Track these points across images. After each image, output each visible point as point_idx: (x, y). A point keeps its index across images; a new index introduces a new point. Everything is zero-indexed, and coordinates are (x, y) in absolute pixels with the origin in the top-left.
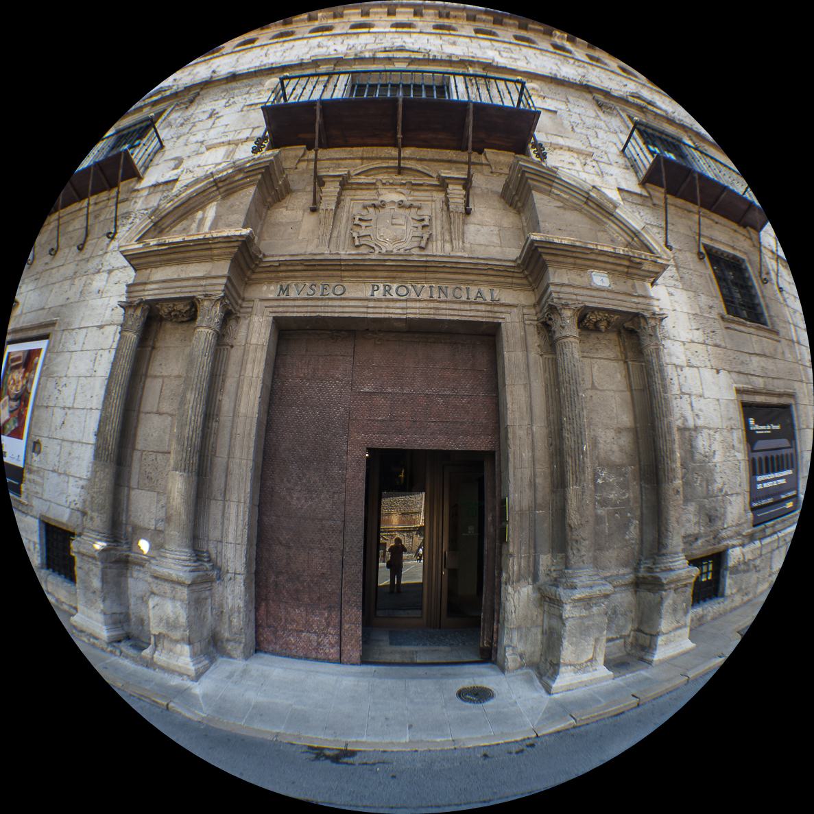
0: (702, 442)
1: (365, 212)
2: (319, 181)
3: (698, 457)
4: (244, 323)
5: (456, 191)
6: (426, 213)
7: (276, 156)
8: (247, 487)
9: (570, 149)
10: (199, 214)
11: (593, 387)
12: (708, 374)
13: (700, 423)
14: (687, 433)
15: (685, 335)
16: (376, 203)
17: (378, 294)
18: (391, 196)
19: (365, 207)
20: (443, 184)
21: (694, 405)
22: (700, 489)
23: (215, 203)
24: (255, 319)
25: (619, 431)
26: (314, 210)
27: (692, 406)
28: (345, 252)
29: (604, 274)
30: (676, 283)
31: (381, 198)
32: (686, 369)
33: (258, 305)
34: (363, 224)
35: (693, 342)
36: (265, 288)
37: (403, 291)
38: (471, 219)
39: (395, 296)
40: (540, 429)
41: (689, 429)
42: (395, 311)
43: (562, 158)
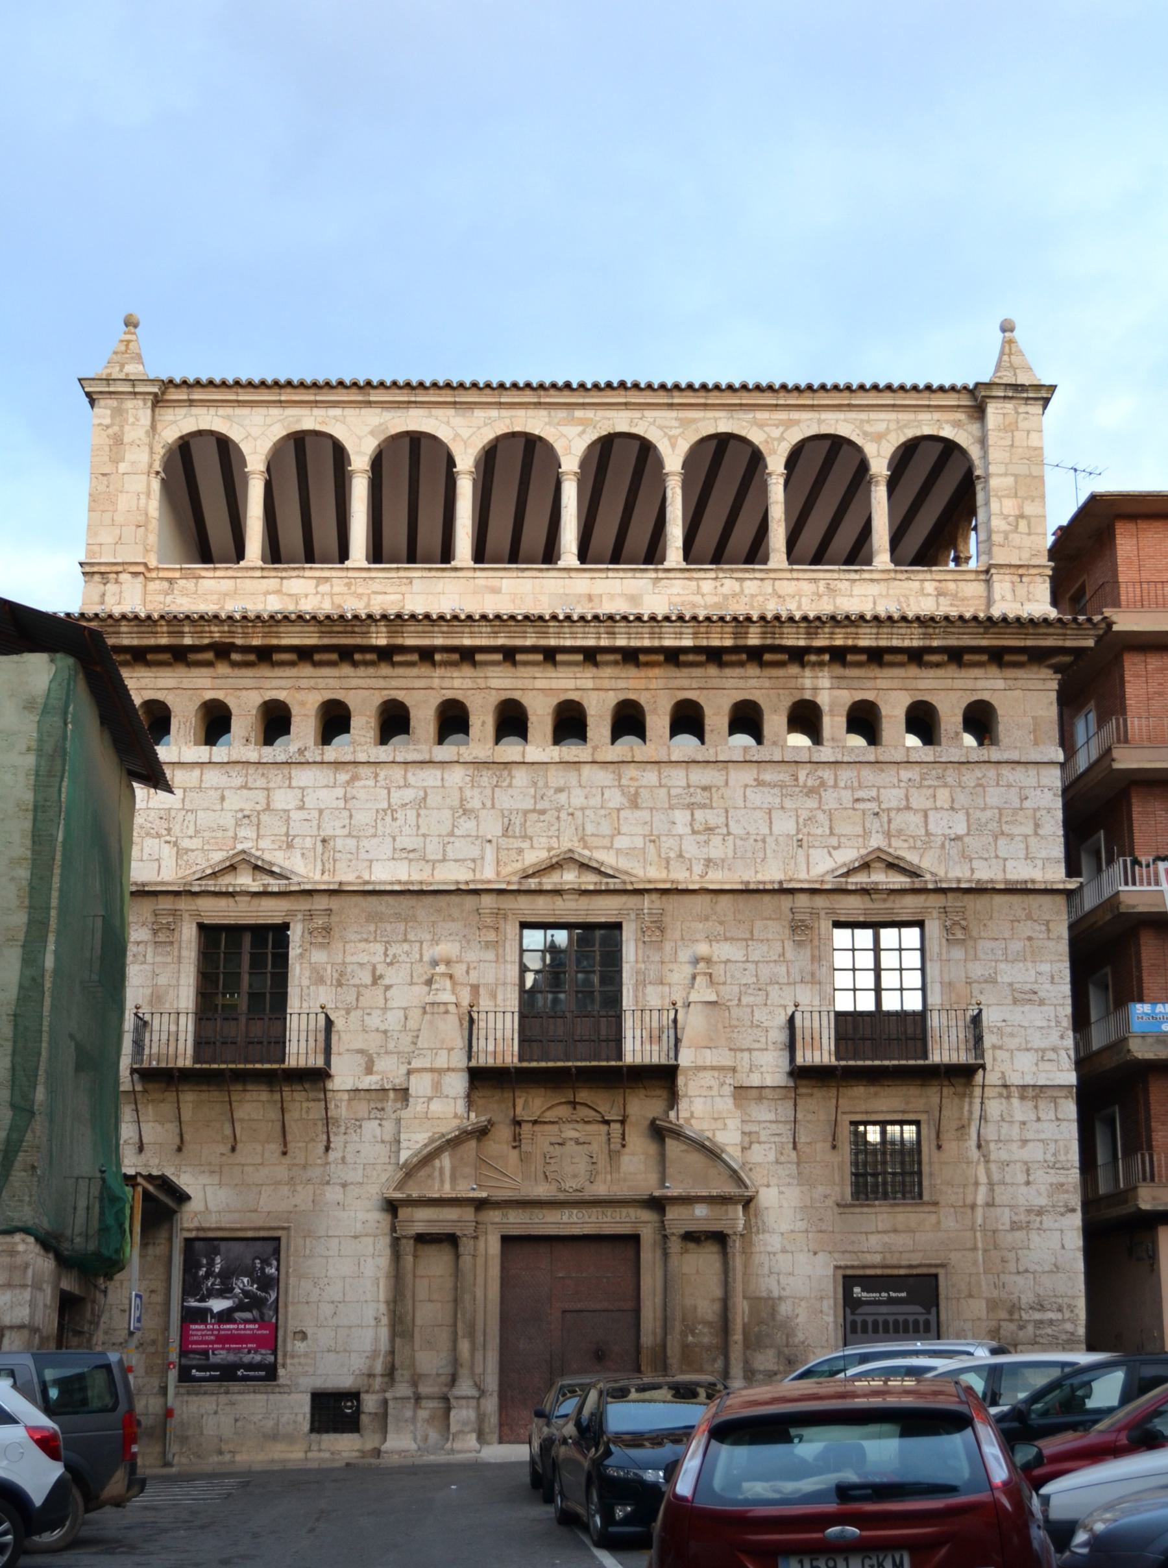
0: (784, 1309)
1: (551, 1149)
2: (517, 1123)
3: (779, 1318)
4: (482, 1239)
5: (616, 1127)
6: (595, 1147)
7: (489, 1121)
8: (497, 1340)
9: (713, 1068)
10: (437, 1163)
11: (698, 1272)
12: (803, 1258)
13: (784, 1294)
14: (770, 1302)
15: (785, 1227)
16: (560, 1141)
17: (565, 1219)
18: (570, 1133)
19: (552, 1144)
20: (607, 1122)
21: (782, 1281)
22: (780, 1338)
23: (447, 1154)
24: (490, 1237)
25: (713, 1300)
26: (515, 1147)
27: (778, 1282)
28: (542, 1191)
29: (704, 1206)
30: (791, 1181)
31: (563, 1135)
32: (780, 1257)
33: (490, 1227)
34: (552, 1161)
35: (792, 1231)
36: (491, 1213)
37: (580, 1215)
38: (626, 1150)
39: (575, 1220)
40: (659, 1300)
41: (773, 1299)
42: (576, 1231)
43: (703, 1082)
